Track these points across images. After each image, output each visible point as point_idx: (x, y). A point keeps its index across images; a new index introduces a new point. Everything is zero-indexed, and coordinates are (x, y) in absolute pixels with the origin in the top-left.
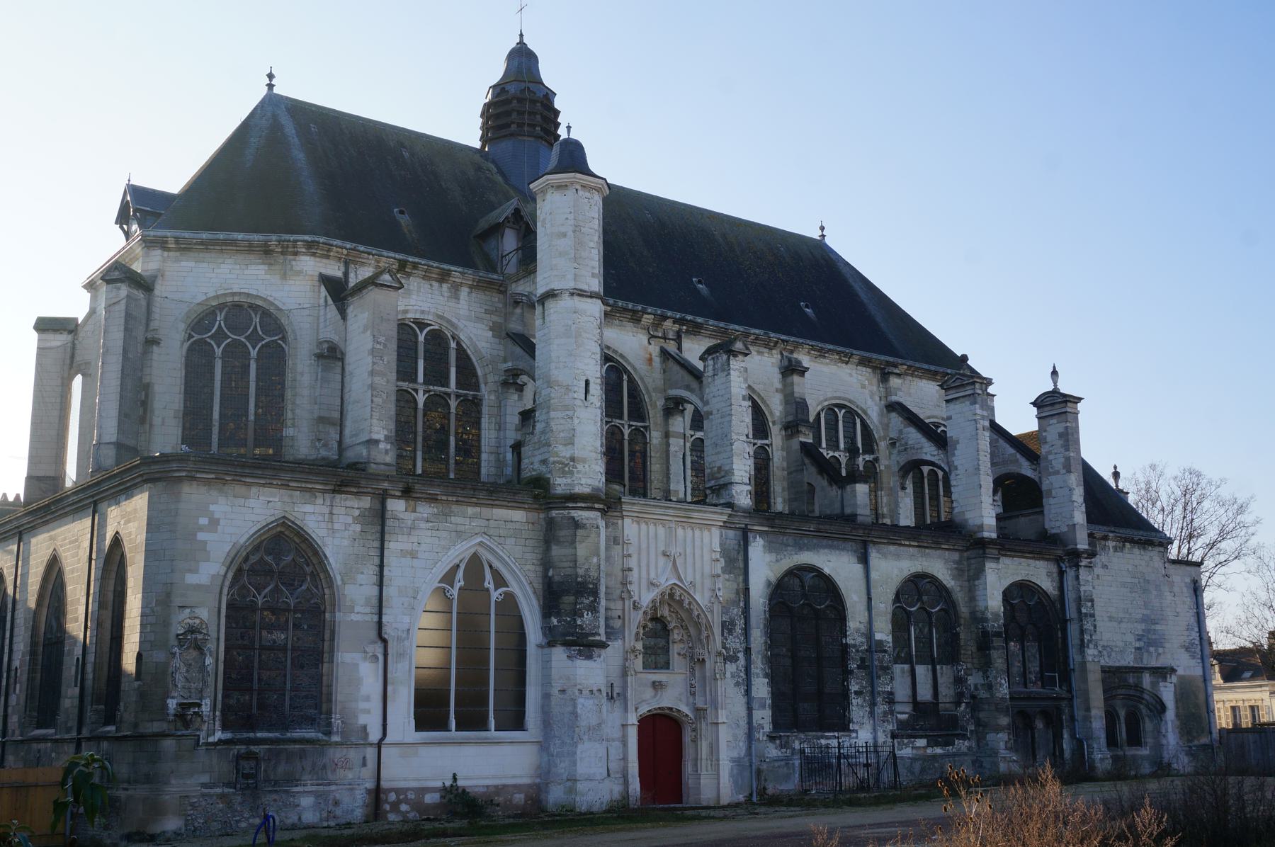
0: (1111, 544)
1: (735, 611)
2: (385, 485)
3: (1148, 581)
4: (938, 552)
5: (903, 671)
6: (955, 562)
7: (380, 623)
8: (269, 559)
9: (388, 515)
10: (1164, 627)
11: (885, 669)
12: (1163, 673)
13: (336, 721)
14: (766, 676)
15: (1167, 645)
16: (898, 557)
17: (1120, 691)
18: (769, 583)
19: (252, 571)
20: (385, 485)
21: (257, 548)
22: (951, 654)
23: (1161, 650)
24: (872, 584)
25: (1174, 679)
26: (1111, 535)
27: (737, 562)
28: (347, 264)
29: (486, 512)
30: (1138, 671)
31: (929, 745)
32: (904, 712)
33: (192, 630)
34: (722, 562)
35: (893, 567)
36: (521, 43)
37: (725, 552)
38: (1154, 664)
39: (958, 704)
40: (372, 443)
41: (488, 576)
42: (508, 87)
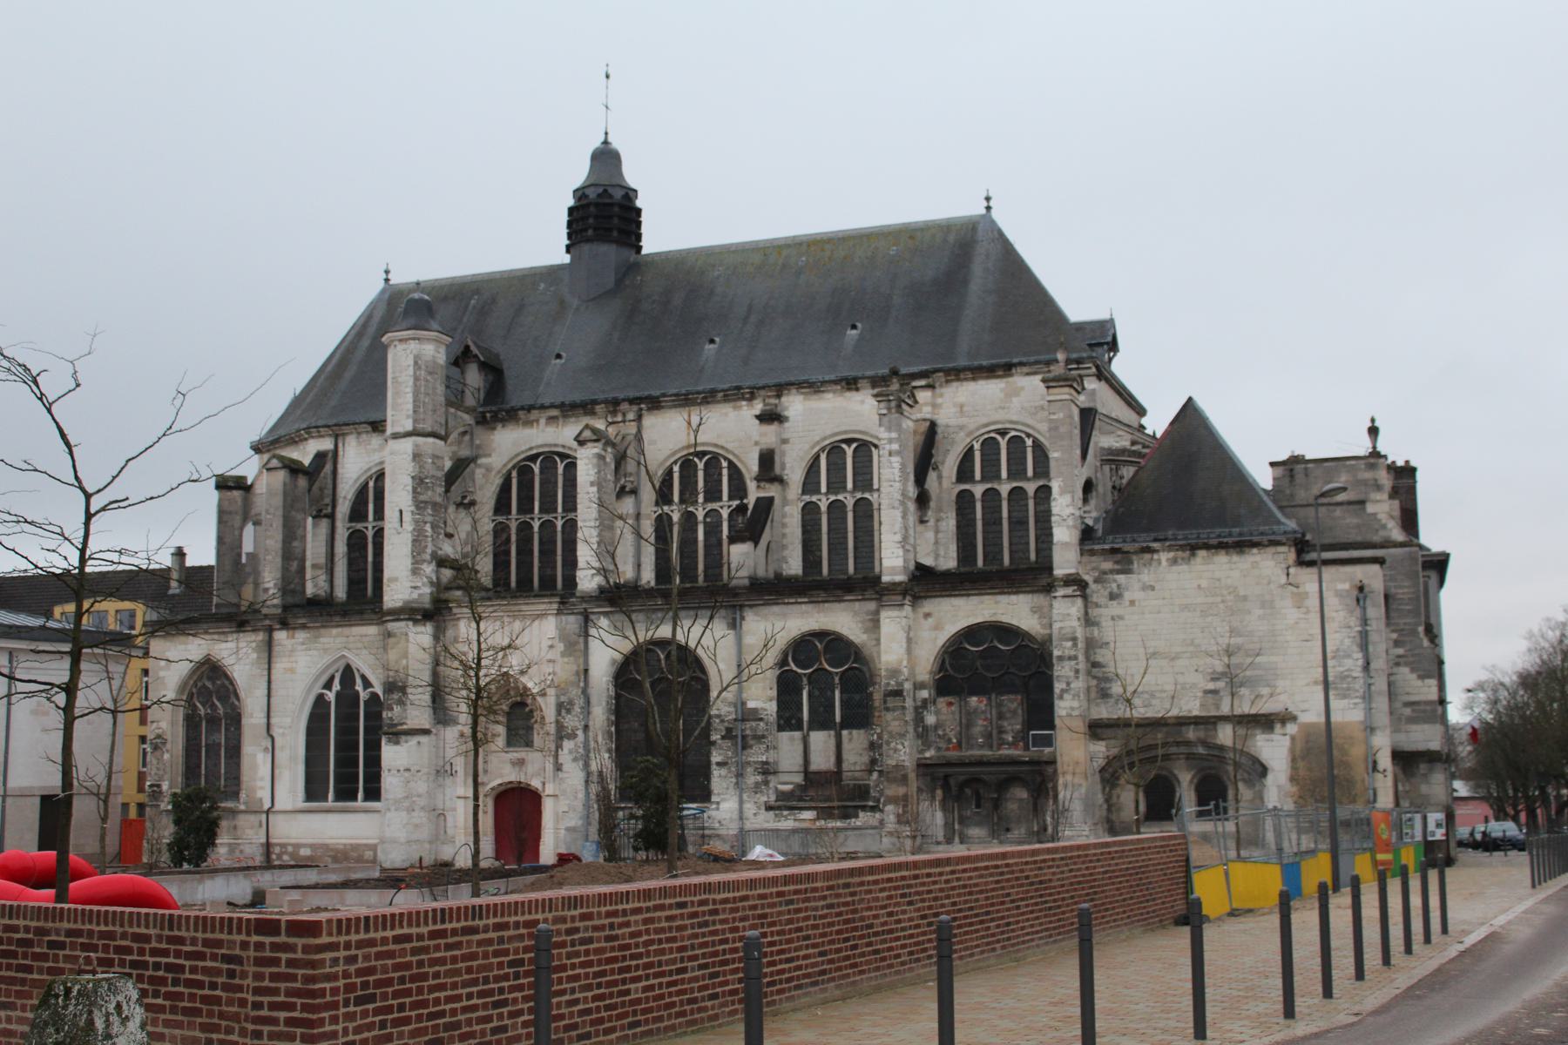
1: (575, 692)
2: (267, 622)
3: (1245, 598)
4: (843, 605)
5: (792, 739)
6: (867, 613)
7: (268, 725)
8: (209, 684)
9: (275, 643)
10: (1273, 659)
11: (760, 738)
12: (1266, 722)
13: (243, 795)
14: (609, 751)
16: (784, 616)
18: (614, 661)
19: (199, 694)
20: (267, 622)
21: (200, 678)
22: (859, 716)
23: (1265, 691)
24: (744, 650)
25: (1291, 728)
26: (1155, 545)
27: (577, 645)
28: (336, 437)
29: (346, 631)
31: (818, 818)
32: (789, 779)
33: (159, 736)
34: (561, 647)
35: (776, 627)
36: (606, 142)
37: (563, 636)
38: (1245, 708)
39: (870, 772)
40: (266, 590)
41: (359, 681)
42: (588, 192)
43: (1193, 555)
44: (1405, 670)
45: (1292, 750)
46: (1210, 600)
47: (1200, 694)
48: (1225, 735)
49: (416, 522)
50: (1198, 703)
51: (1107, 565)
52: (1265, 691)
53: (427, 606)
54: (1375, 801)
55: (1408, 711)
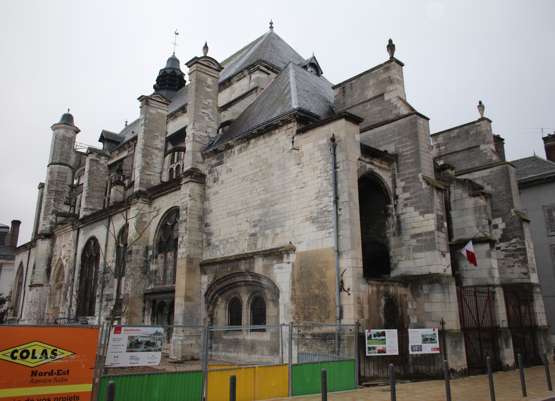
0: (237, 148)
10: (284, 205)
12: (277, 254)
15: (288, 223)
17: (238, 279)
25: (293, 258)
30: (249, 257)
38: (269, 245)
43: (249, 144)
44: (411, 209)
45: (293, 275)
46: (255, 171)
47: (248, 238)
48: (259, 266)
49: (48, 198)
50: (246, 244)
51: (214, 162)
52: (278, 230)
53: (48, 232)
54: (341, 317)
55: (414, 242)
